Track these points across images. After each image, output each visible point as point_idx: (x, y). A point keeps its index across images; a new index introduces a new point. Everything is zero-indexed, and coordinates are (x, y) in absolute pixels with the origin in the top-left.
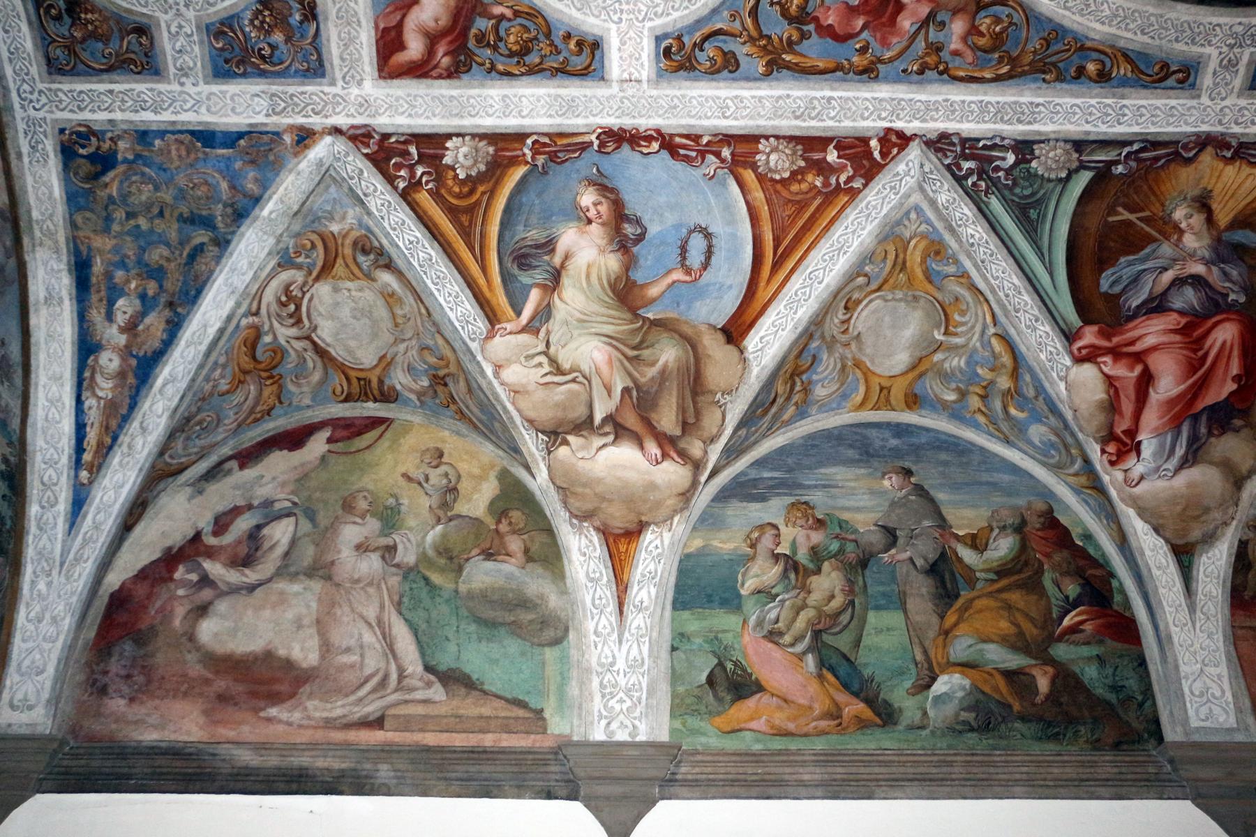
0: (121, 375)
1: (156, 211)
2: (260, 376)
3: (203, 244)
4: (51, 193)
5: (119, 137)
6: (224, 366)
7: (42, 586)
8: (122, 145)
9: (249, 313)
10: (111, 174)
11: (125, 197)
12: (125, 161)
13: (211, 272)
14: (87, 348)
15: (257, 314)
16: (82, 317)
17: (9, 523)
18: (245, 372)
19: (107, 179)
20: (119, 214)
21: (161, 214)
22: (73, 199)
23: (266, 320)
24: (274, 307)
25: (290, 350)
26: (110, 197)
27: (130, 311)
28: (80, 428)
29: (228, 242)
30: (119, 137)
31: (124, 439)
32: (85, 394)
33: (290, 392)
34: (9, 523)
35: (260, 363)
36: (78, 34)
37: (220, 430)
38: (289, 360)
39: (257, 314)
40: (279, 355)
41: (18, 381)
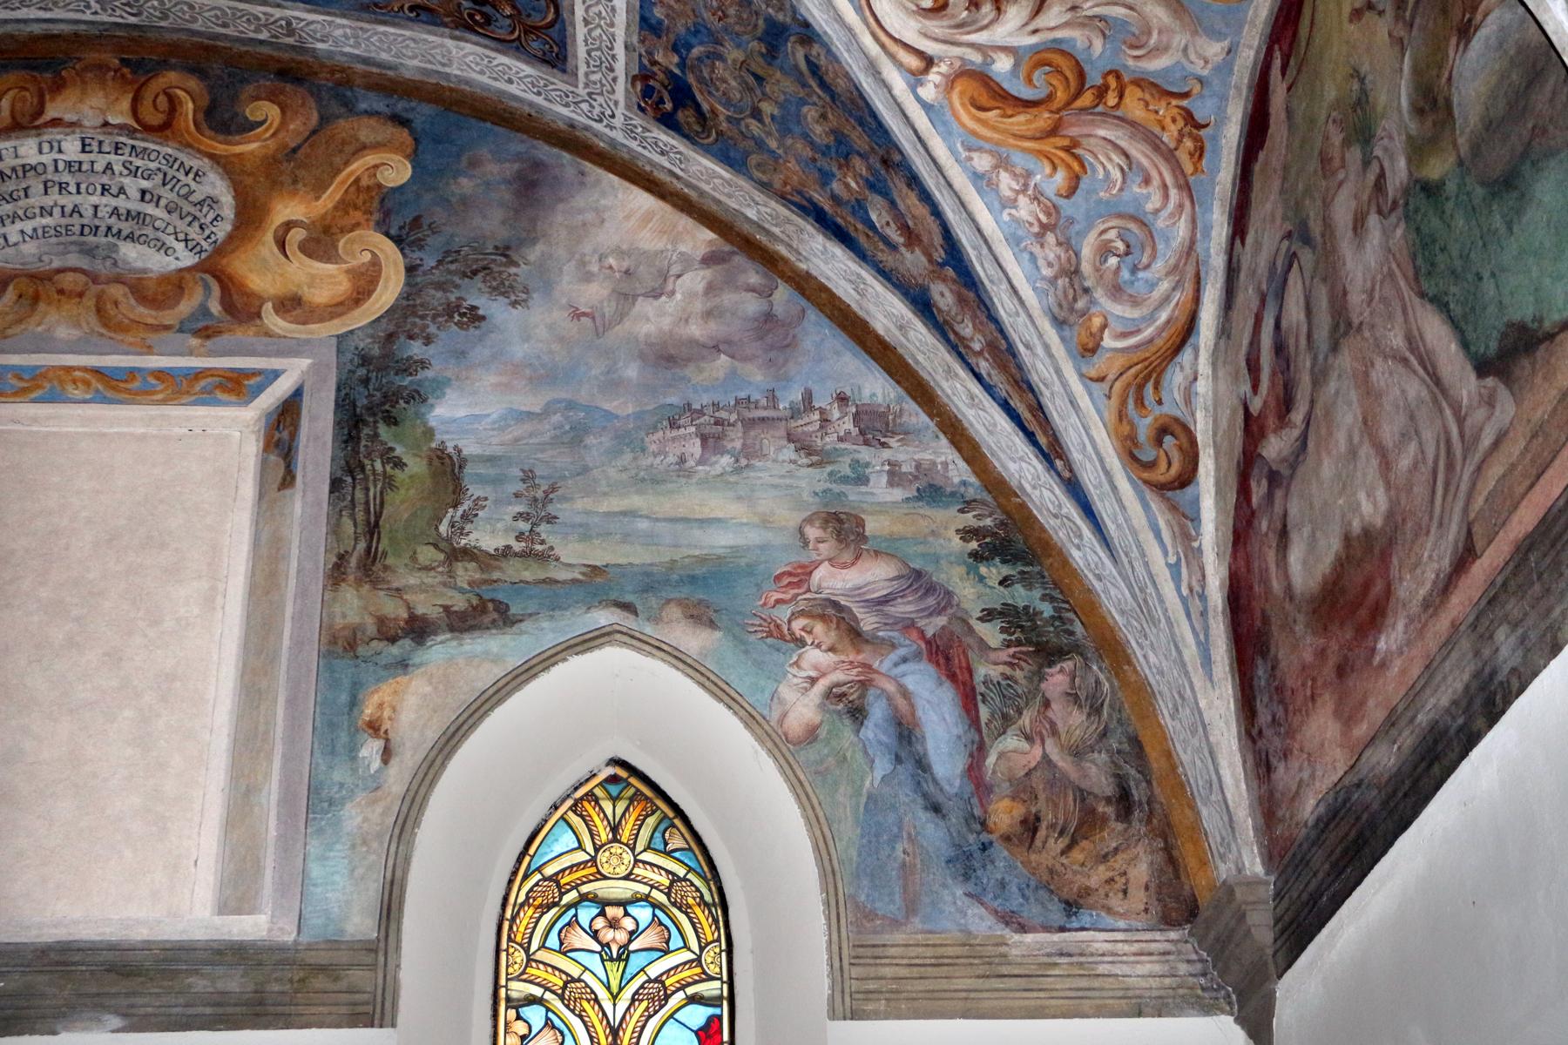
0: (961, 300)
1: (751, 80)
2: (1083, 110)
3: (806, 57)
4: (722, 178)
5: (650, 53)
6: (1003, 163)
7: (1152, 658)
8: (659, 57)
9: (916, 78)
10: (699, 97)
11: (728, 103)
12: (682, 65)
13: (847, 75)
14: (923, 305)
15: (929, 62)
16: (885, 274)
17: (1047, 610)
18: (1053, 131)
19: (705, 107)
20: (755, 127)
21: (759, 79)
22: (726, 159)
23: (957, 51)
24: (936, 26)
25: (1059, 34)
26: (729, 119)
27: (886, 217)
28: (1006, 407)
29: (807, 25)
30: (650, 53)
31: (1034, 378)
32: (973, 360)
33: (1166, 70)
34: (1047, 610)
35: (1050, 97)
36: (508, 11)
37: (1160, 223)
38: (1081, 43)
39: (929, 62)
40: (1058, 59)
41: (916, 416)
